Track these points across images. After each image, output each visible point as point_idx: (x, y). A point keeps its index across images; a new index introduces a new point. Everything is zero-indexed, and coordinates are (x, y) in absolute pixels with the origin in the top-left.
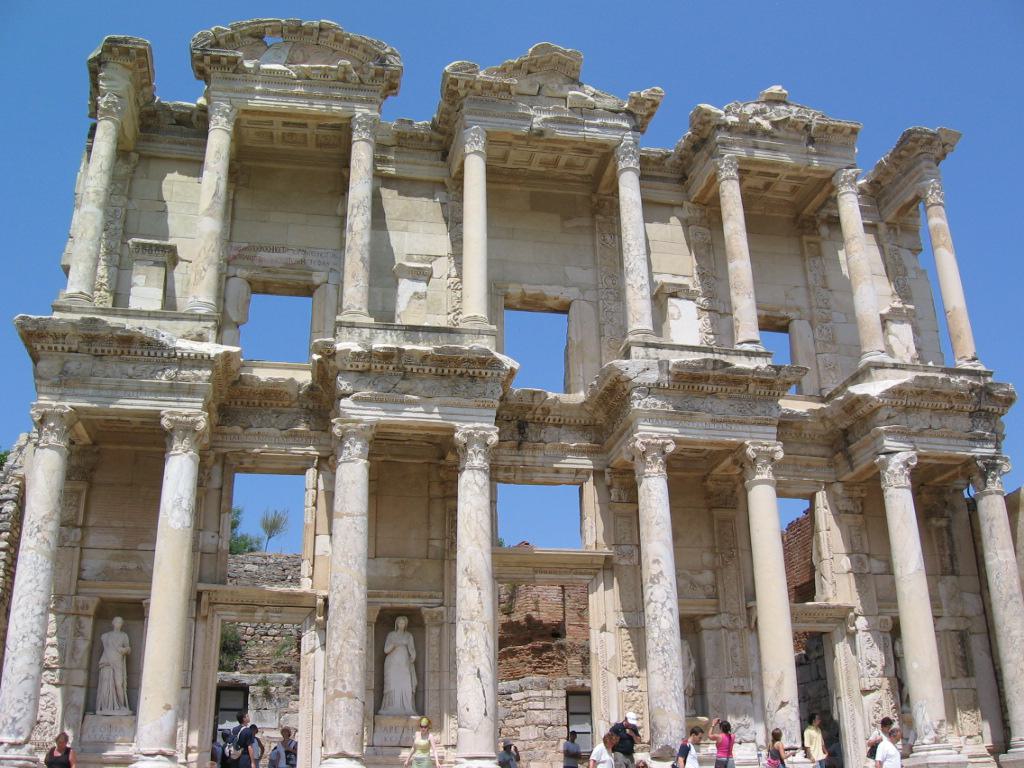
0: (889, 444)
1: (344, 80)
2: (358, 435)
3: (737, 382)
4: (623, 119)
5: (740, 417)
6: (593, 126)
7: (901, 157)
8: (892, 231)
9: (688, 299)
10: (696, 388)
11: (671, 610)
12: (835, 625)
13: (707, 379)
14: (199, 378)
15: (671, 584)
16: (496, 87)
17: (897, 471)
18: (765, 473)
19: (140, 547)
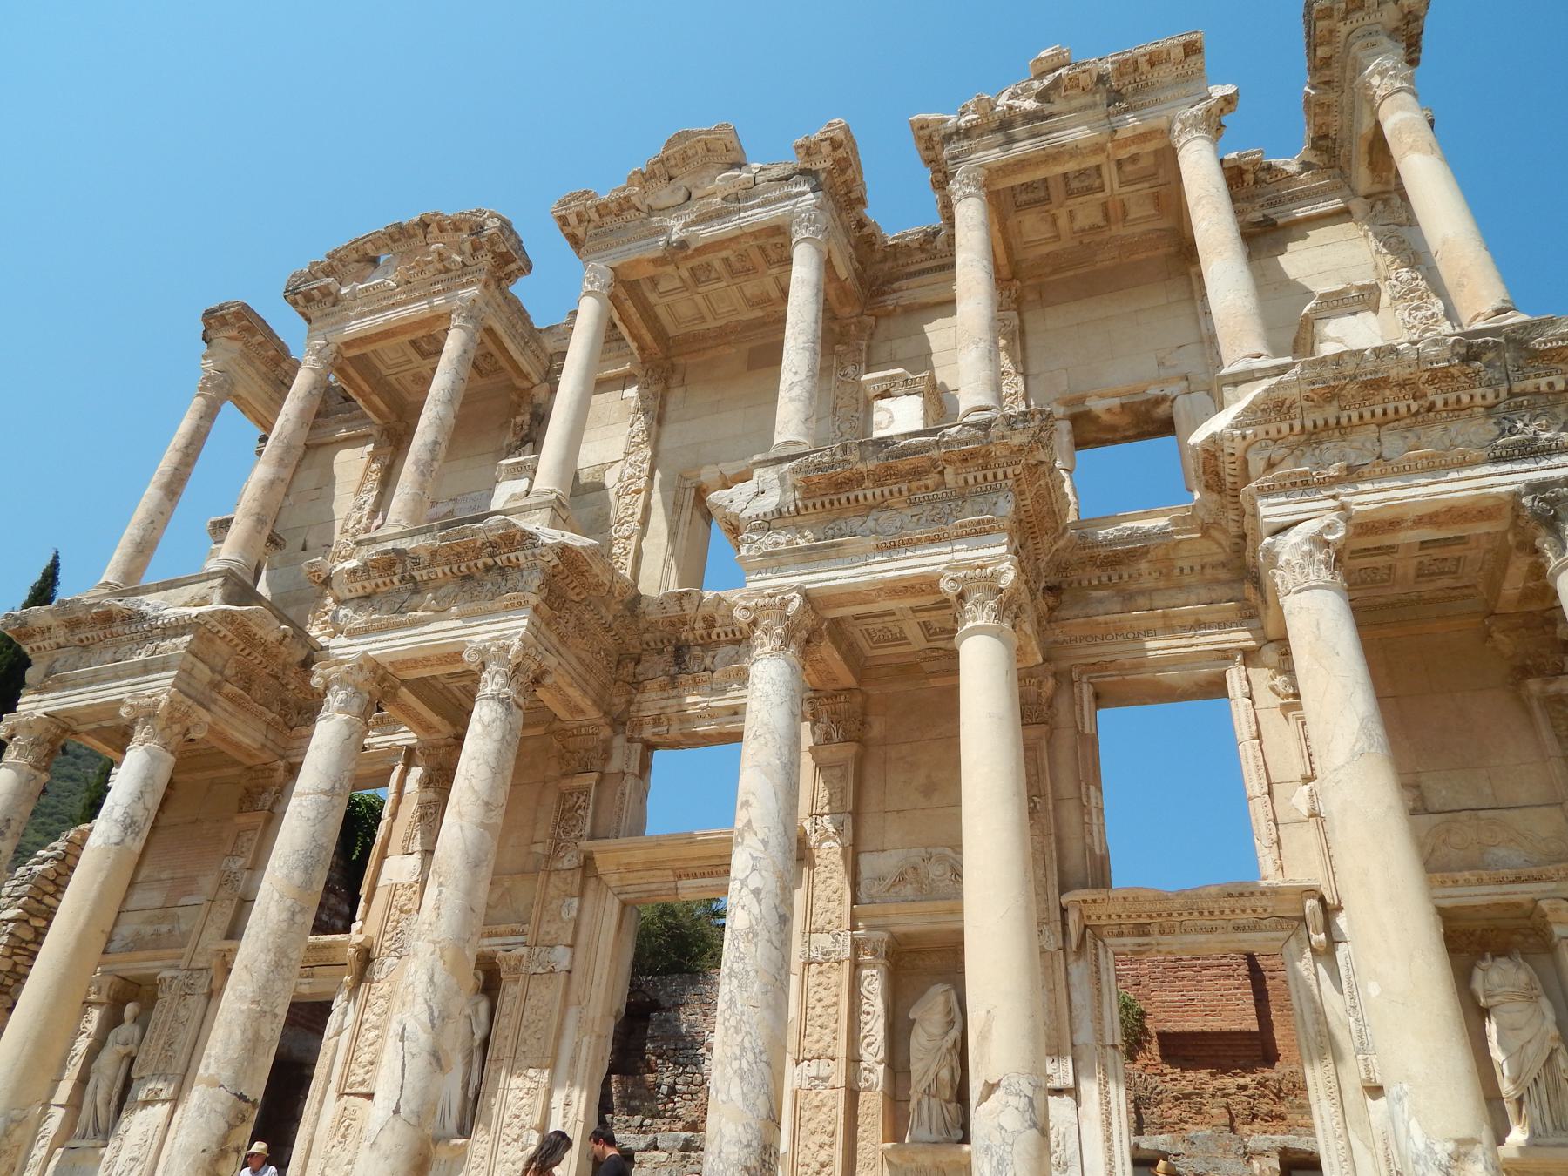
0: (1270, 510)
1: (447, 270)
2: (342, 682)
3: (918, 473)
4: (796, 184)
5: (934, 530)
6: (752, 207)
7: (1327, 62)
8: (1379, 206)
9: (908, 394)
10: (844, 501)
11: (756, 892)
12: (1284, 934)
13: (858, 480)
14: (177, 648)
15: (765, 843)
16: (613, 206)
17: (1296, 560)
18: (979, 615)
19: (183, 901)
